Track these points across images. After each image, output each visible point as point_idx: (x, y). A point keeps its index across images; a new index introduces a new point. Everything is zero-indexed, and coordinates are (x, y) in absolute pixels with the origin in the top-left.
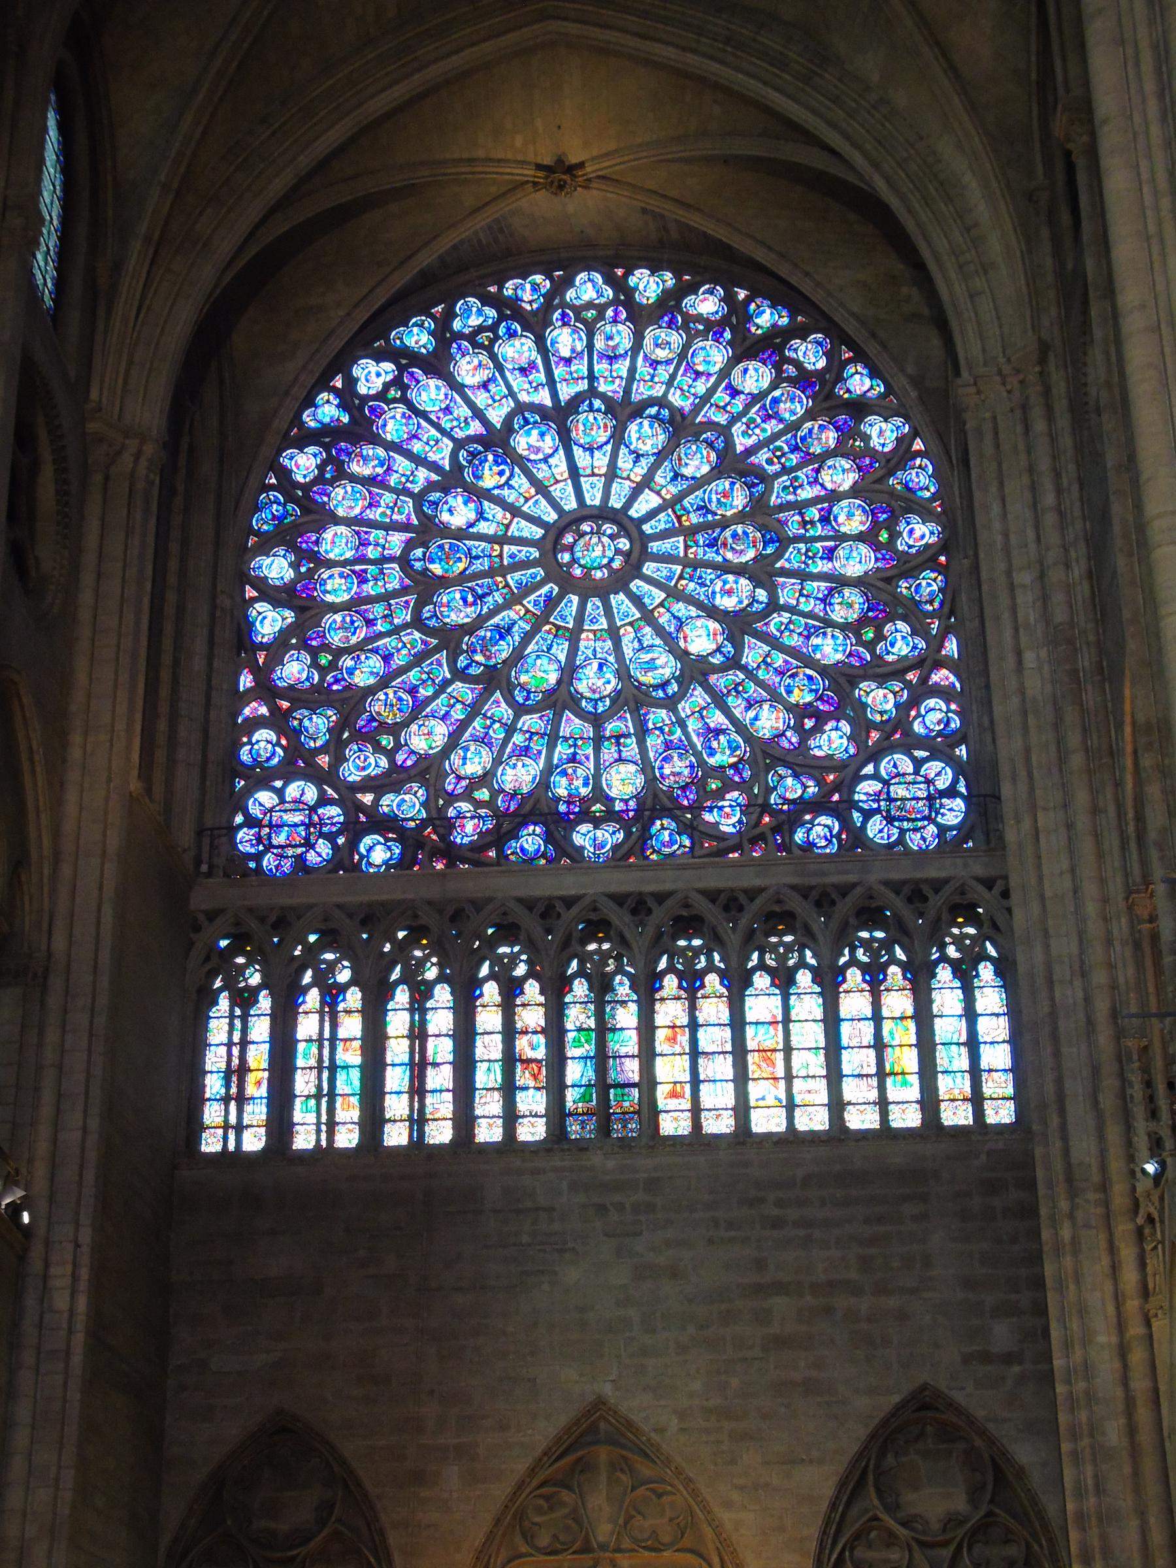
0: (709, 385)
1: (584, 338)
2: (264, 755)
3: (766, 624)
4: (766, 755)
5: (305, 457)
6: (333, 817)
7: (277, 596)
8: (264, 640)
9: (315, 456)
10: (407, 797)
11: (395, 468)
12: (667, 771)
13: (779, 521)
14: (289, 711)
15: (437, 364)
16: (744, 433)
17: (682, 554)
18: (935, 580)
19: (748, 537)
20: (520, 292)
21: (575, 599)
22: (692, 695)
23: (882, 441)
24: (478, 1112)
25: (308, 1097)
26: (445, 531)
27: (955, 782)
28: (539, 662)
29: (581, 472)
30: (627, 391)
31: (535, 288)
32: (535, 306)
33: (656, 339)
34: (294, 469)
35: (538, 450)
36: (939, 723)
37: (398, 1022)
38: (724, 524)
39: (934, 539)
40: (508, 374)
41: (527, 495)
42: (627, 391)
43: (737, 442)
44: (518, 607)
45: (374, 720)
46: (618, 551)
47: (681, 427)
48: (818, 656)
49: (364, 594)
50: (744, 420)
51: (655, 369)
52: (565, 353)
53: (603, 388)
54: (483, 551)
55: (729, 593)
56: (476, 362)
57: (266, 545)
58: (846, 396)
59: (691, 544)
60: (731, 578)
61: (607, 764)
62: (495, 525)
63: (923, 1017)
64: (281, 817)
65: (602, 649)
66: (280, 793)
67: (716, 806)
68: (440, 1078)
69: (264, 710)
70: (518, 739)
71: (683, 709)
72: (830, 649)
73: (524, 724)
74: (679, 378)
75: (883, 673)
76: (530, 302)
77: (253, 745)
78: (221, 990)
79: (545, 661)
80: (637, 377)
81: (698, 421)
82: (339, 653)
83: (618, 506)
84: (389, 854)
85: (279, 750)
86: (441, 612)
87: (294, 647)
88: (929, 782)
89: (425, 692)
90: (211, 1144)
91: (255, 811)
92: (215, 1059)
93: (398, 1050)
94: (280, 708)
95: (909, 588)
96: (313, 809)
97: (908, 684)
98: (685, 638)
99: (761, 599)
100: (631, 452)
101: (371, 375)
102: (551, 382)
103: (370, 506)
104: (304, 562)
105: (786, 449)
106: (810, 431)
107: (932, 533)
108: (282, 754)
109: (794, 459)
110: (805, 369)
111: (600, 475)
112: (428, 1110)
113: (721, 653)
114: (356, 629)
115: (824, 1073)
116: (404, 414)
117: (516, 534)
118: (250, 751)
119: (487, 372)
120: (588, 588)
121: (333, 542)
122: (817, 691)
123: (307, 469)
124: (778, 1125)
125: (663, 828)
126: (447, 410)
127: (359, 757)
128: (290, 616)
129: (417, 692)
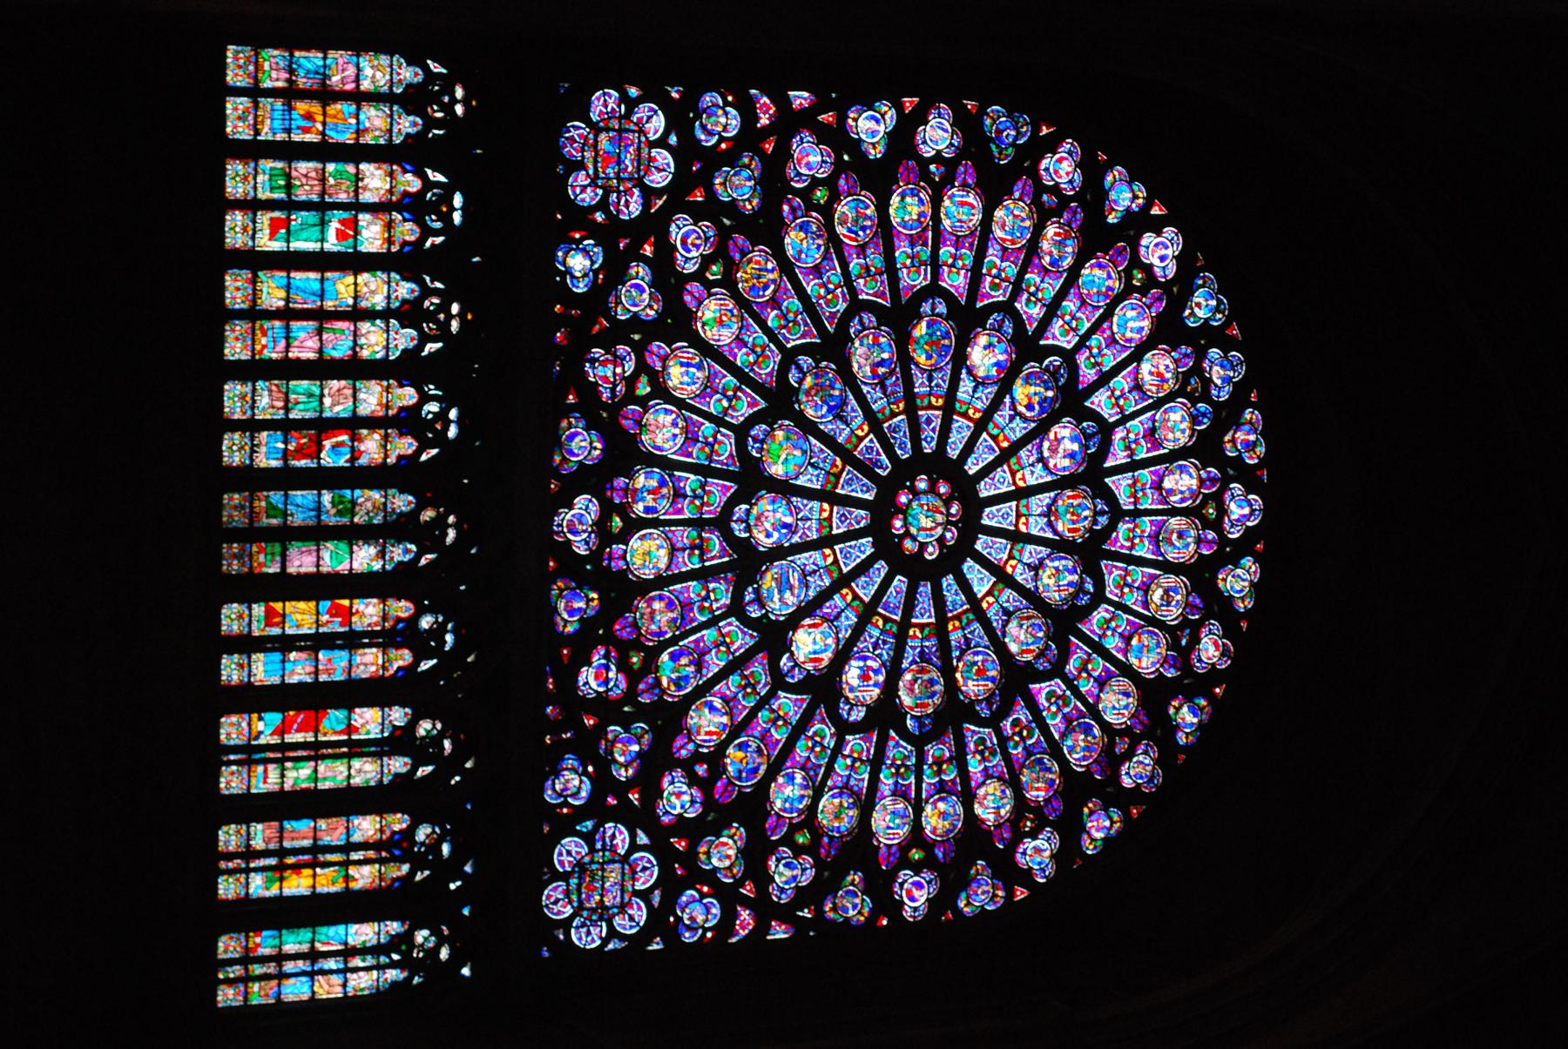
4: (668, 719)
7: (903, 138)
9: (1071, 182)
10: (646, 296)
12: (657, 605)
13: (944, 733)
14: (761, 154)
15: (1168, 331)
20: (1247, 427)
21: (869, 496)
22: (744, 633)
24: (260, 384)
25: (288, 177)
26: (964, 341)
27: (622, 937)
28: (797, 453)
29: (1024, 502)
31: (1250, 446)
32: (1229, 446)
35: (1053, 450)
36: (692, 919)
37: (376, 289)
38: (948, 671)
39: (907, 913)
40: (1149, 415)
44: (866, 428)
45: (743, 254)
46: (923, 546)
47: (1063, 622)
48: (781, 780)
52: (1168, 483)
53: (1123, 528)
54: (938, 385)
55: (864, 677)
56: (1168, 375)
57: (967, 125)
58: (1086, 810)
59: (926, 631)
60: (881, 678)
63: (349, 907)
66: (662, 143)
68: (305, 347)
69: (764, 120)
70: (708, 428)
71: (730, 624)
72: (787, 794)
75: (755, 857)
76: (1233, 441)
78: (426, 69)
79: (799, 461)
82: (827, 211)
83: (978, 546)
84: (578, 274)
85: (715, 140)
87: (839, 158)
88: (623, 908)
89: (772, 319)
90: (236, 66)
91: (642, 111)
92: (341, 68)
93: (342, 288)
96: (639, 183)
97: (739, 883)
98: (815, 626)
100: (1041, 561)
101: (1161, 251)
103: (1004, 249)
105: (1029, 742)
106: (1049, 770)
107: (915, 909)
110: (1123, 764)
111: (1016, 525)
112: (267, 324)
113: (793, 668)
115: (287, 787)
116: (1112, 289)
117: (956, 425)
118: (717, 106)
119: (1154, 389)
120: (883, 509)
121: (963, 204)
123: (1056, 172)
124: (228, 734)
126: (1112, 341)
127: (699, 238)
128: (875, 153)
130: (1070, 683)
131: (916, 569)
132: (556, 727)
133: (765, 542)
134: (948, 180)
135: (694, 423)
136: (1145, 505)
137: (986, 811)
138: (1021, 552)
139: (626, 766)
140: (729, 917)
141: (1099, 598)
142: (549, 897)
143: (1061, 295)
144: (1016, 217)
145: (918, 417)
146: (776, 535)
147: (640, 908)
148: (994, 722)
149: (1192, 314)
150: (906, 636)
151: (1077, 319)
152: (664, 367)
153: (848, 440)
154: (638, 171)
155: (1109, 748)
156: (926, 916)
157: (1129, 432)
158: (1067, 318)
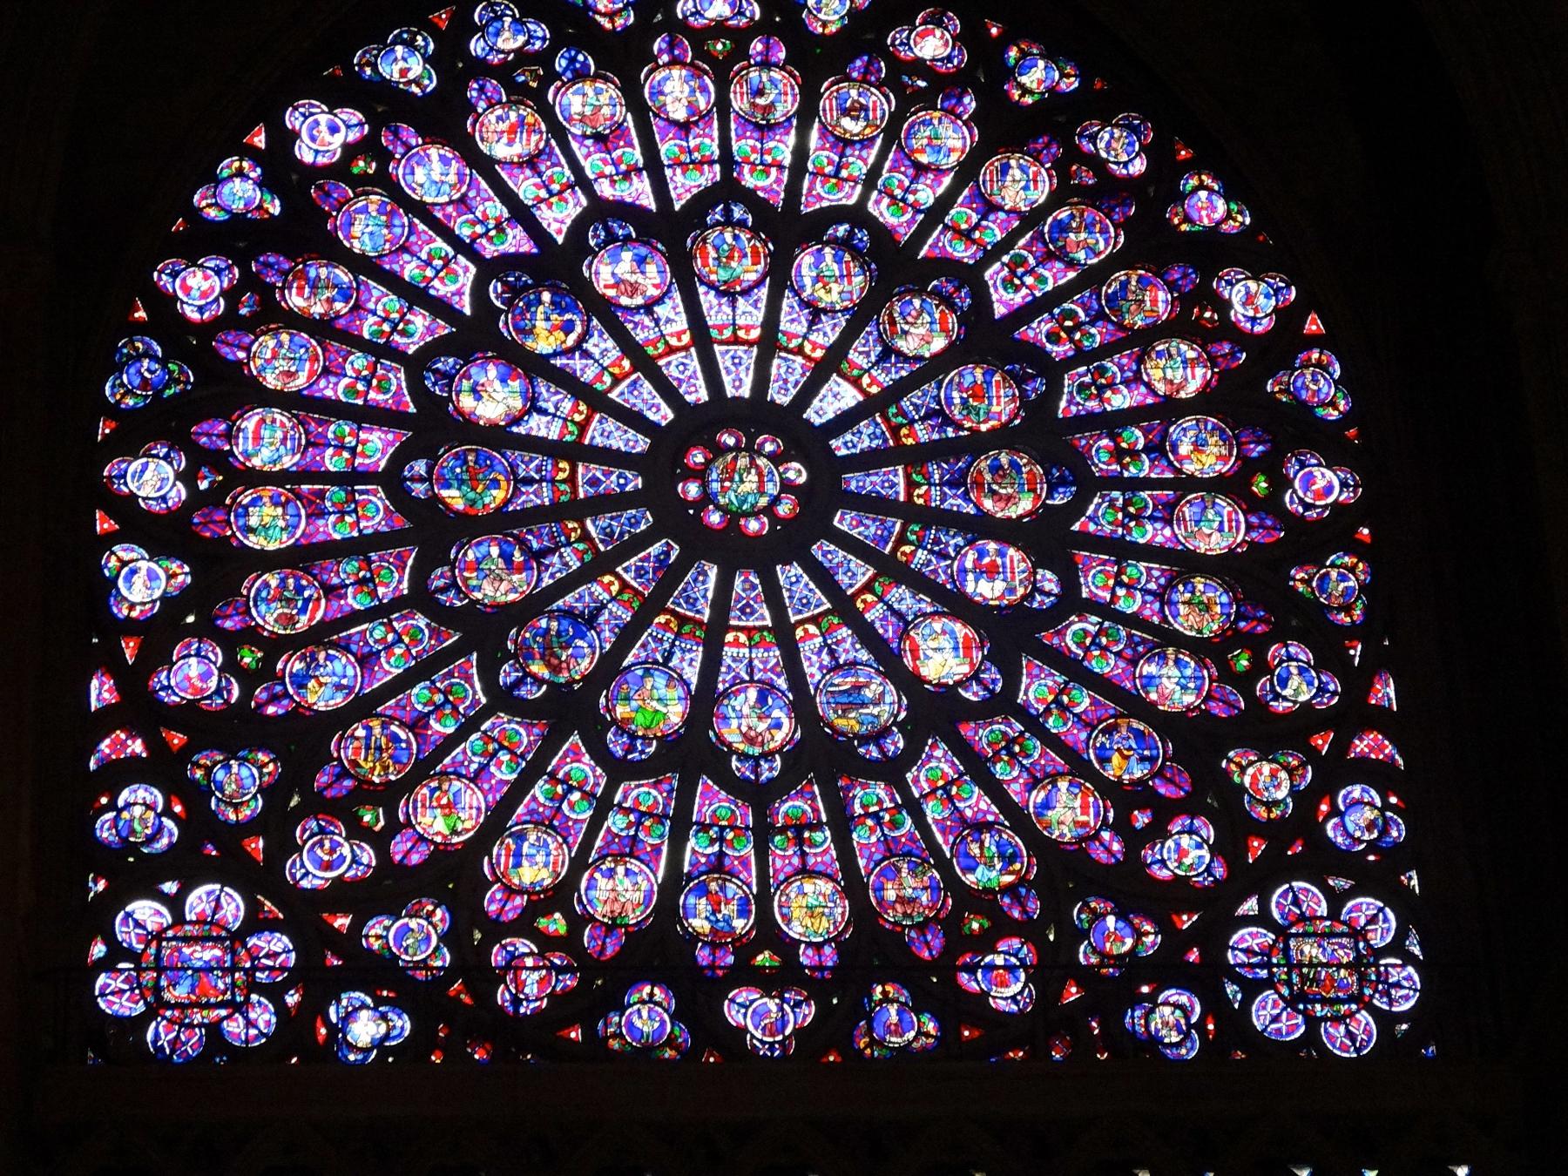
0: (940, 191)
1: (712, 88)
2: (142, 832)
3: (1058, 633)
4: (1063, 871)
5: (199, 274)
6: (275, 955)
7: (159, 532)
8: (134, 614)
10: (413, 923)
11: (371, 305)
12: (891, 895)
13: (1074, 448)
15: (444, 120)
16: (1007, 283)
17: (902, 498)
18: (1352, 569)
19: (1019, 472)
21: (713, 572)
22: (930, 757)
23: (1251, 313)
27: (1401, 935)
29: (714, 333)
30: (793, 190)
32: (619, 22)
33: (841, 100)
34: (180, 294)
35: (634, 289)
36: (1371, 826)
38: (977, 444)
40: (574, 145)
41: (616, 371)
42: (793, 190)
43: (995, 297)
44: (607, 579)
45: (344, 774)
46: (787, 486)
47: (895, 268)
48: (1153, 696)
49: (321, 537)
50: (1006, 259)
51: (842, 156)
52: (680, 114)
53: (750, 180)
54: (538, 470)
55: (991, 572)
56: (513, 116)
57: (135, 435)
58: (1184, 227)
59: (918, 478)
60: (992, 546)
61: (781, 877)
62: (558, 423)
64: (179, 950)
65: (765, 662)
66: (175, 904)
67: (978, 965)
69: (137, 747)
70: (616, 822)
71: (916, 780)
72: (1174, 685)
73: (625, 798)
74: (885, 174)
76: (610, 16)
77: (120, 811)
79: (660, 681)
80: (810, 167)
81: (922, 254)
82: (275, 646)
83: (784, 400)
84: (383, 1029)
85: (168, 823)
86: (465, 580)
87: (192, 631)
88: (1357, 934)
89: (445, 727)
91: (126, 934)
94: (165, 744)
95: (1307, 582)
96: (239, 937)
97: (1312, 755)
99: (1048, 586)
100: (805, 304)
101: (322, 134)
102: (654, 167)
103: (326, 372)
104: (204, 470)
106: (1124, 285)
107: (1344, 484)
108: (176, 831)
109: (1096, 336)
110: (1111, 174)
111: (750, 343)
113: (980, 682)
114: (307, 601)
117: (599, 441)
119: (535, 138)
120: (733, 550)
121: (258, 438)
122: (1152, 760)
123: (204, 295)
125: (886, 998)
127: (321, 844)
129: (427, 726)
130: (991, 255)
131: (823, 496)
132: (1082, 1044)
133: (785, 731)
134: (220, 461)
135: (608, 844)
136: (714, 149)
137: (1194, 381)
138: (791, 336)
139: (1139, 935)
140: (1368, 772)
141: (857, 215)
142: (1343, 1048)
143: (394, 283)
144: (275, 356)
145: (587, 498)
146: (776, 713)
147: (1357, 908)
148: (1054, 371)
149: (417, 82)
150: (927, 507)
151: (431, 257)
152: (521, 891)
153: (627, 605)
154: (218, 940)
155: (1090, 197)
156: (1353, 469)
157: (601, 175)
158: (429, 273)
